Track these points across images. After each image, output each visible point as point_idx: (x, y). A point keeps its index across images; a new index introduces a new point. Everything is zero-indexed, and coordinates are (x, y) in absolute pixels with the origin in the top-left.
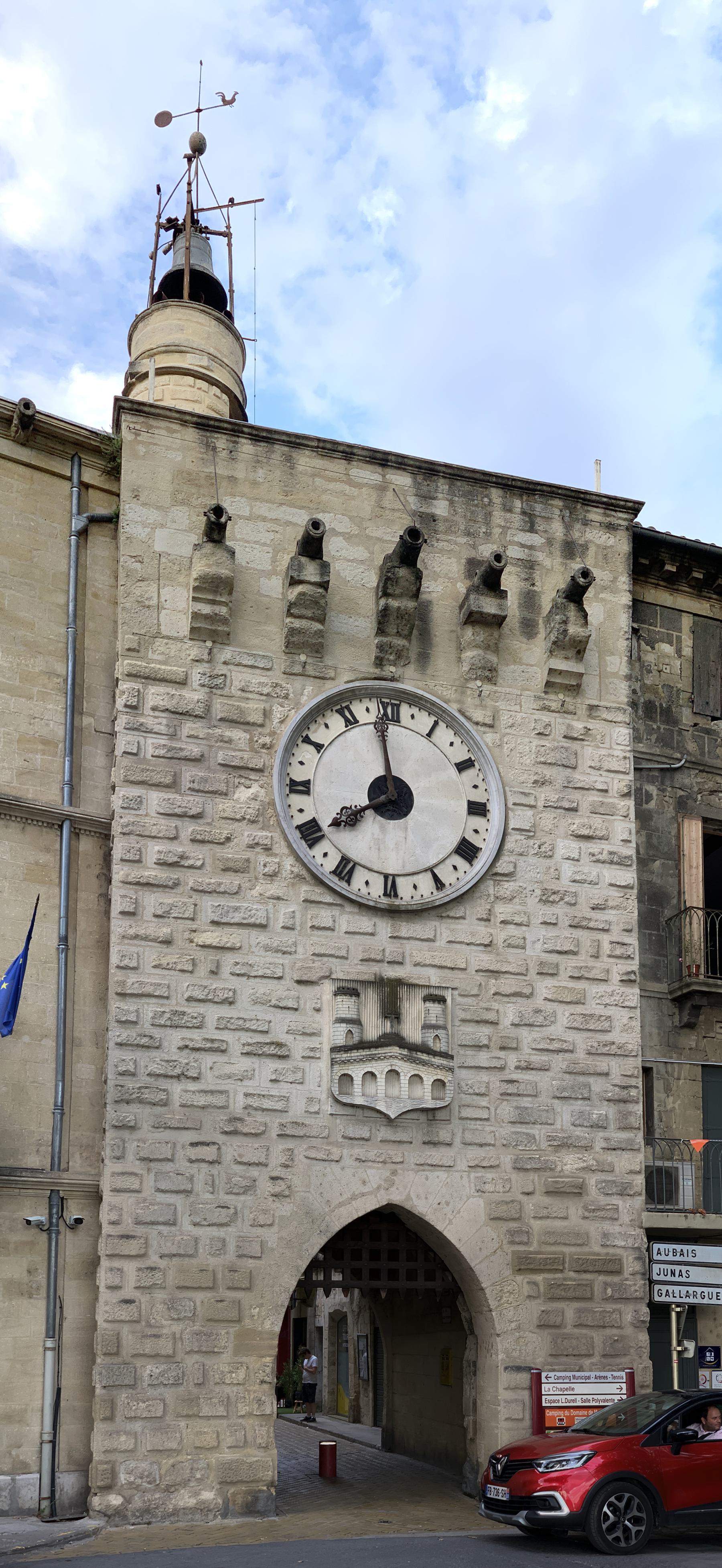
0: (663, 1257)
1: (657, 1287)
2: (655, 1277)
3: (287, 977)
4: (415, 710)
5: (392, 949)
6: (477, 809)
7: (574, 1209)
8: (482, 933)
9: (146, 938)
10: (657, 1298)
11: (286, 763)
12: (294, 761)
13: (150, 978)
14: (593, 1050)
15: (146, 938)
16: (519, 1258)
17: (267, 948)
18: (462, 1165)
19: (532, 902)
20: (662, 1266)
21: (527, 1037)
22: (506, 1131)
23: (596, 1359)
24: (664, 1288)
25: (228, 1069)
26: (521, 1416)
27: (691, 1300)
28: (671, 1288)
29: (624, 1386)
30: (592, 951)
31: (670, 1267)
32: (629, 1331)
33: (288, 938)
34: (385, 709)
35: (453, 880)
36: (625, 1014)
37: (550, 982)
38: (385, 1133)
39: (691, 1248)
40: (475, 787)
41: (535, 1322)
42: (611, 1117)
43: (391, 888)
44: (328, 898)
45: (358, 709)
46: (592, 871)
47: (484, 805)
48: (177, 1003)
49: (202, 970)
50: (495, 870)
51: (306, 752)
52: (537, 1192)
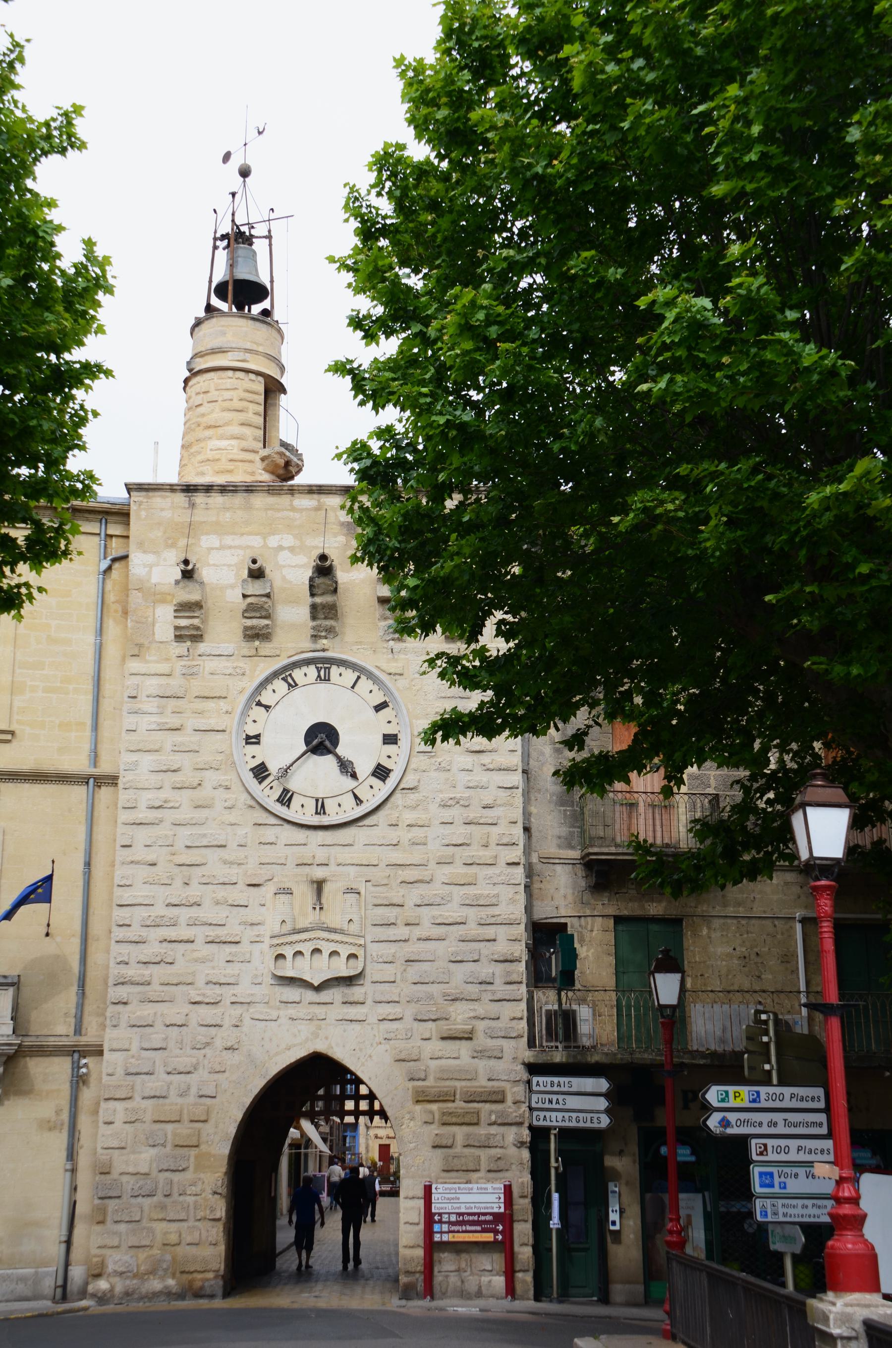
0: (542, 1088)
1: (535, 1113)
2: (534, 1105)
3: (240, 882)
4: (342, 669)
5: (321, 855)
6: (390, 739)
7: (464, 1049)
8: (393, 835)
9: (137, 863)
10: (535, 1123)
11: (242, 722)
12: (249, 720)
13: (138, 893)
14: (483, 922)
15: (137, 863)
16: (417, 1092)
17: (225, 862)
18: (372, 1019)
19: (433, 808)
20: (540, 1096)
21: (426, 913)
22: (409, 990)
23: (482, 1174)
24: (542, 1114)
25: (196, 955)
26: (416, 1221)
27: (567, 1124)
28: (548, 1114)
29: (502, 1196)
30: (484, 842)
31: (547, 1096)
32: (512, 1151)
33: (241, 854)
34: (319, 672)
35: (369, 797)
36: (511, 890)
37: (447, 869)
38: (310, 995)
39: (566, 1080)
40: (389, 722)
41: (430, 1144)
42: (497, 974)
43: (321, 809)
44: (273, 821)
45: (298, 674)
46: (483, 778)
47: (396, 735)
48: (160, 910)
49: (178, 883)
50: (402, 786)
51: (258, 712)
52: (434, 1037)
